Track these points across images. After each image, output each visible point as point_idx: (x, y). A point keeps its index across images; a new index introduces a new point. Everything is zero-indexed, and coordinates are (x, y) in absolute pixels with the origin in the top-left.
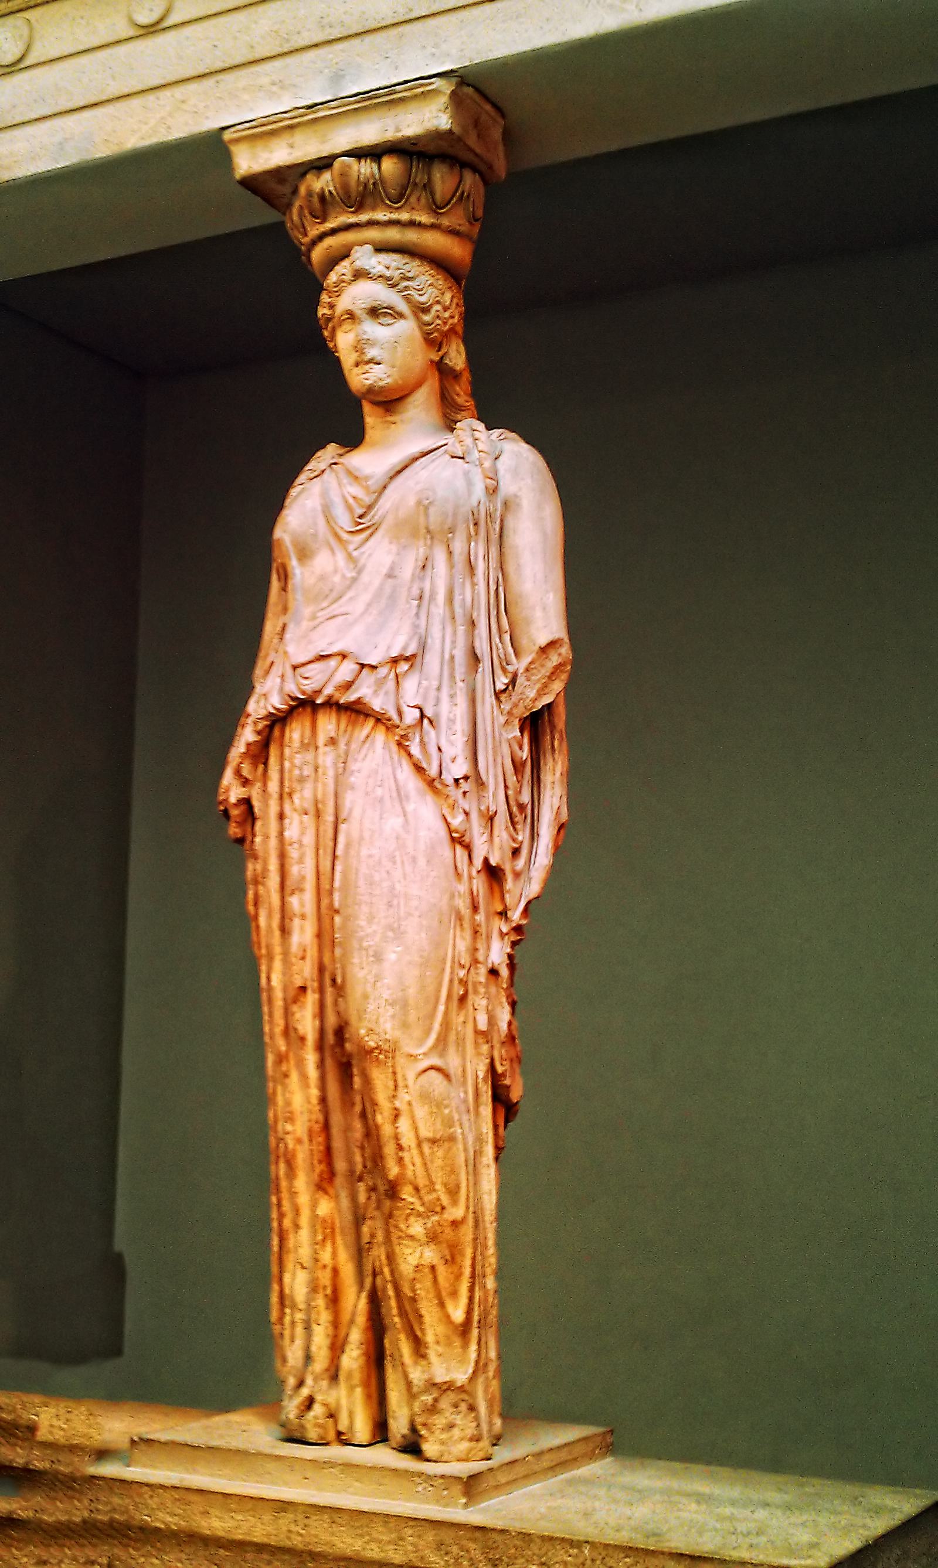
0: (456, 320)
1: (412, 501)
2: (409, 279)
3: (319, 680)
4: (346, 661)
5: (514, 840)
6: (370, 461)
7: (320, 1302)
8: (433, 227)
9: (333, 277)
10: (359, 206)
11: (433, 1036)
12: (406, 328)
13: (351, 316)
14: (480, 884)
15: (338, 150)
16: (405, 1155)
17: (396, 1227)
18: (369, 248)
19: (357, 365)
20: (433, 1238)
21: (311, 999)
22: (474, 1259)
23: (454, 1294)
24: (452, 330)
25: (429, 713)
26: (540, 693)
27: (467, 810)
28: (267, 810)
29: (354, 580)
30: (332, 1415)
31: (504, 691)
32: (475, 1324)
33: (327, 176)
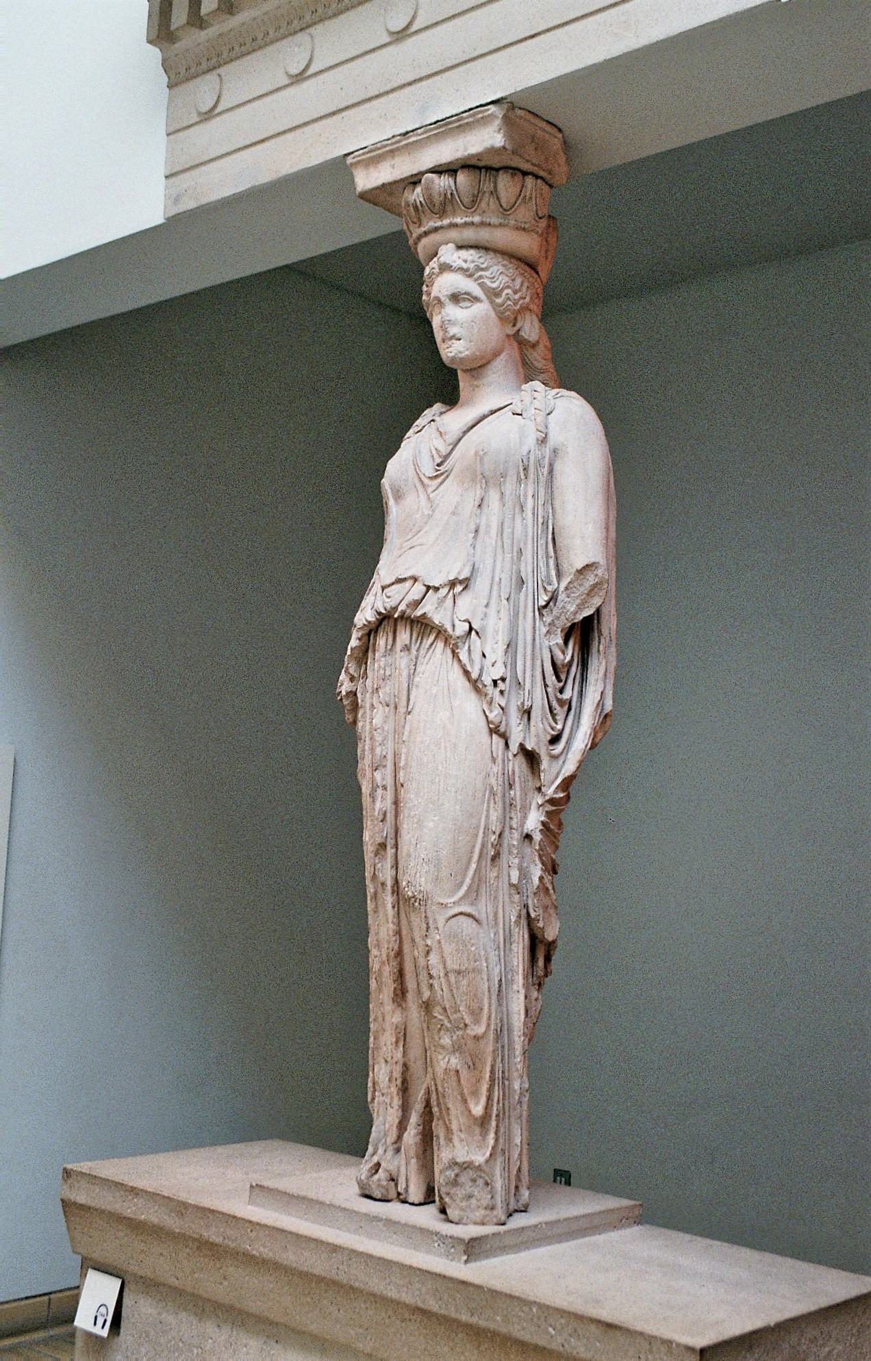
0: (528, 299)
1: (472, 452)
2: (482, 269)
3: (399, 598)
5: (553, 729)
6: (455, 420)
10: (442, 213)
11: (465, 888)
12: (482, 309)
14: (518, 766)
15: (424, 169)
18: (451, 246)
20: (457, 1048)
22: (493, 1066)
23: (475, 1093)
24: (525, 309)
26: (580, 608)
27: (503, 705)
28: (365, 699)
29: (430, 516)
32: (494, 1117)
33: (418, 190)
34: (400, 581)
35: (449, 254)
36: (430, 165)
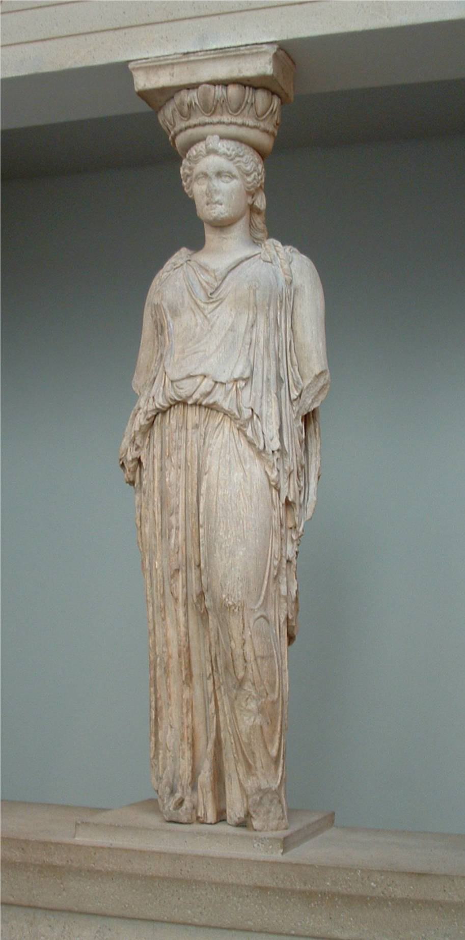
4: (206, 380)
7: (186, 747)
8: (255, 127)
9: (193, 152)
13: (205, 175)
16: (249, 666)
17: (240, 705)
18: (217, 137)
19: (208, 204)
21: (181, 576)
25: (257, 411)
29: (209, 331)
30: (195, 808)
31: (295, 400)
34: (190, 377)
35: (213, 142)
36: (208, 79)
